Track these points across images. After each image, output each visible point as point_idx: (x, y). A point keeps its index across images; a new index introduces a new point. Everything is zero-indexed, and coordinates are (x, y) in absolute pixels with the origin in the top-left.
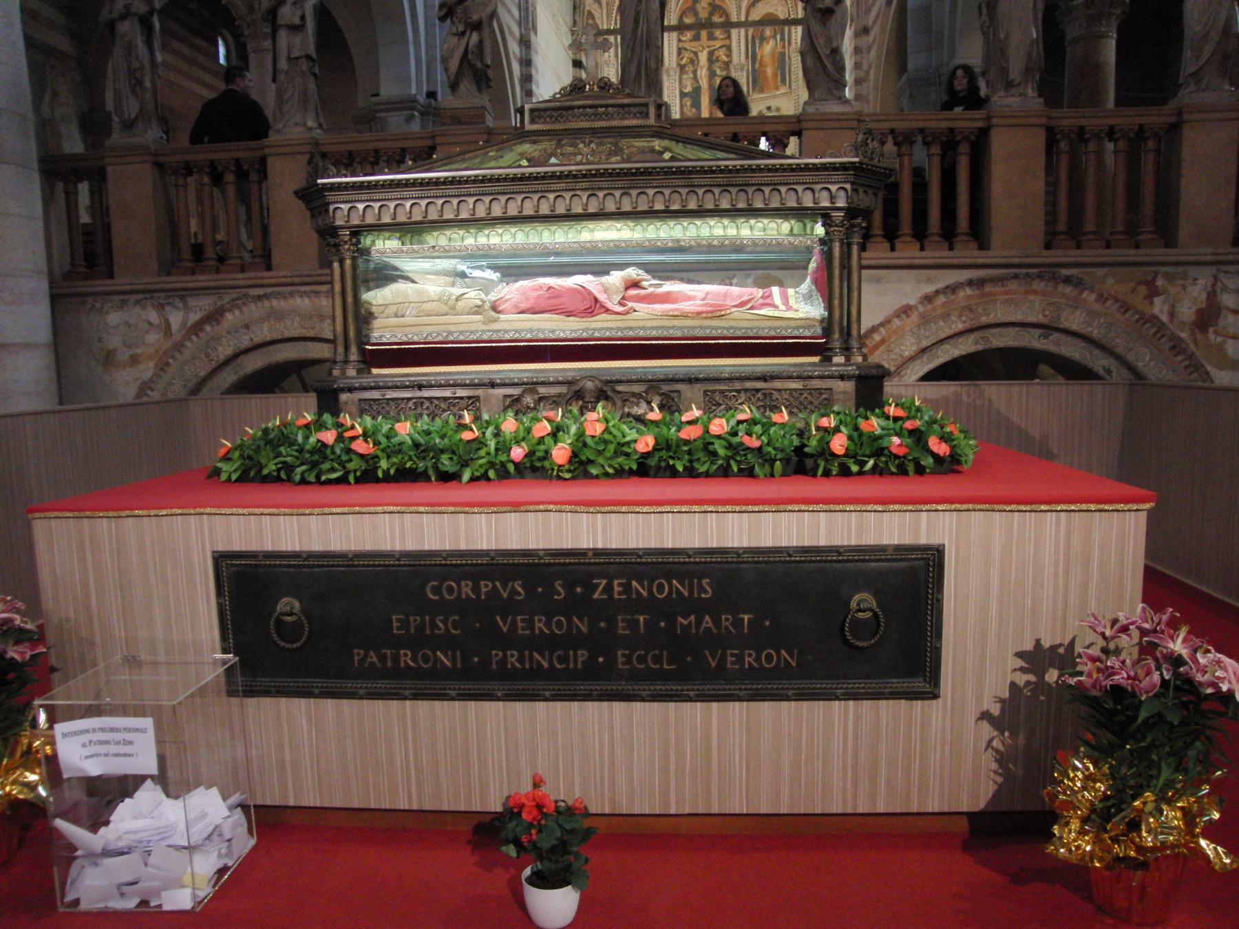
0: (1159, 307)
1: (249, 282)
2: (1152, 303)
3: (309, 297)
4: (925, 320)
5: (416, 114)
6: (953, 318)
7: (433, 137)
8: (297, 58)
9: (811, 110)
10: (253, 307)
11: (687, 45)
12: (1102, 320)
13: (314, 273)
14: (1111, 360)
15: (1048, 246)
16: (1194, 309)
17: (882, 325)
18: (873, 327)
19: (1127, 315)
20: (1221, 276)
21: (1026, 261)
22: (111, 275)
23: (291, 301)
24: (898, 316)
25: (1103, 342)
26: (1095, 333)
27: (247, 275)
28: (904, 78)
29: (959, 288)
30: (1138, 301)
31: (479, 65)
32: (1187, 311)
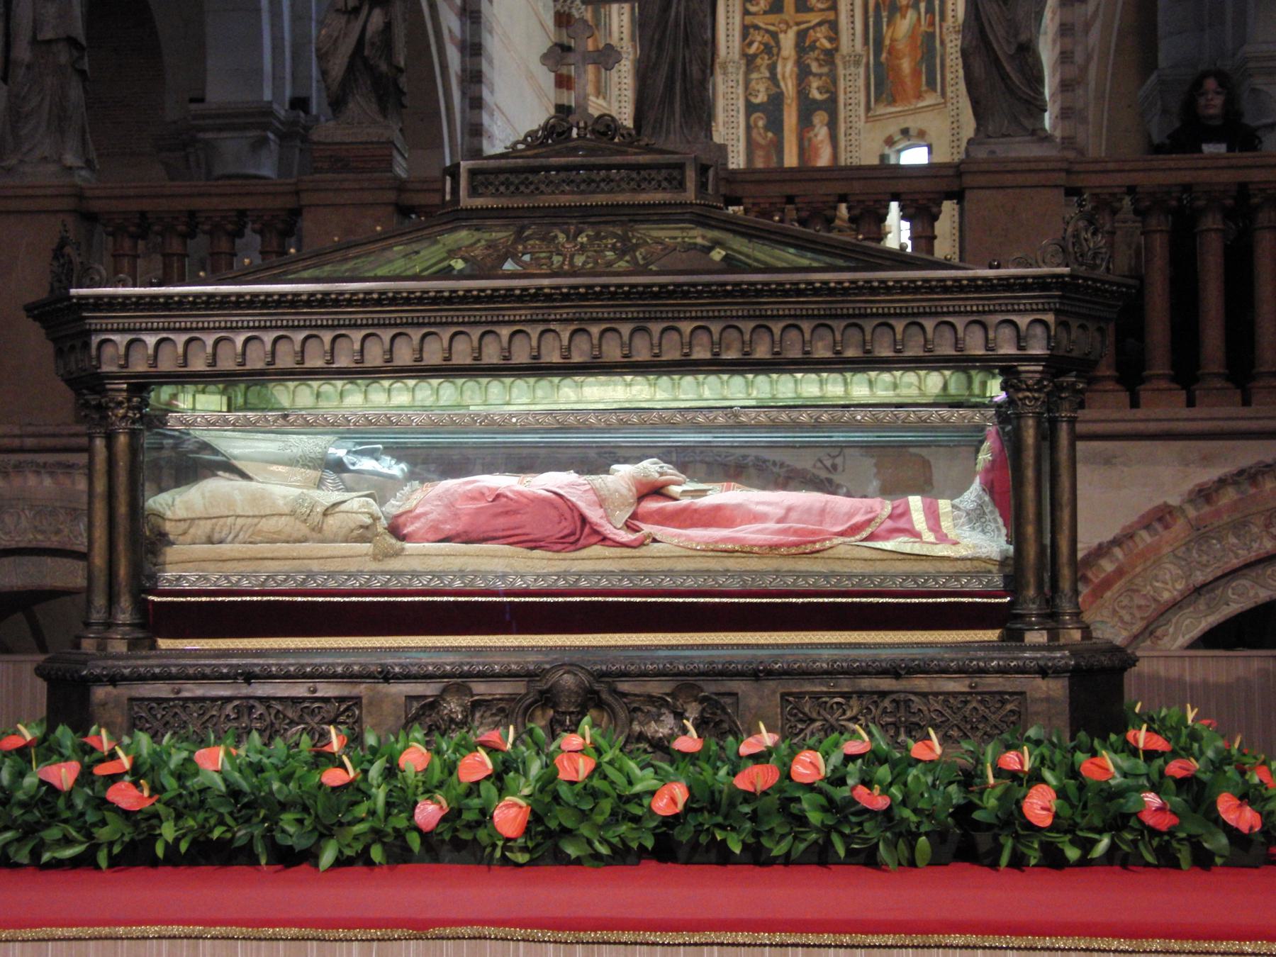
3: (52, 474)
4: (1201, 534)
5: (271, 136)
6: (1255, 530)
7: (297, 193)
8: (49, 42)
9: (981, 153)
11: (759, 21)
17: (1116, 542)
18: (1100, 546)
23: (17, 481)
24: (1147, 527)
28: (1153, 77)
29: (1263, 473)
31: (384, 67)
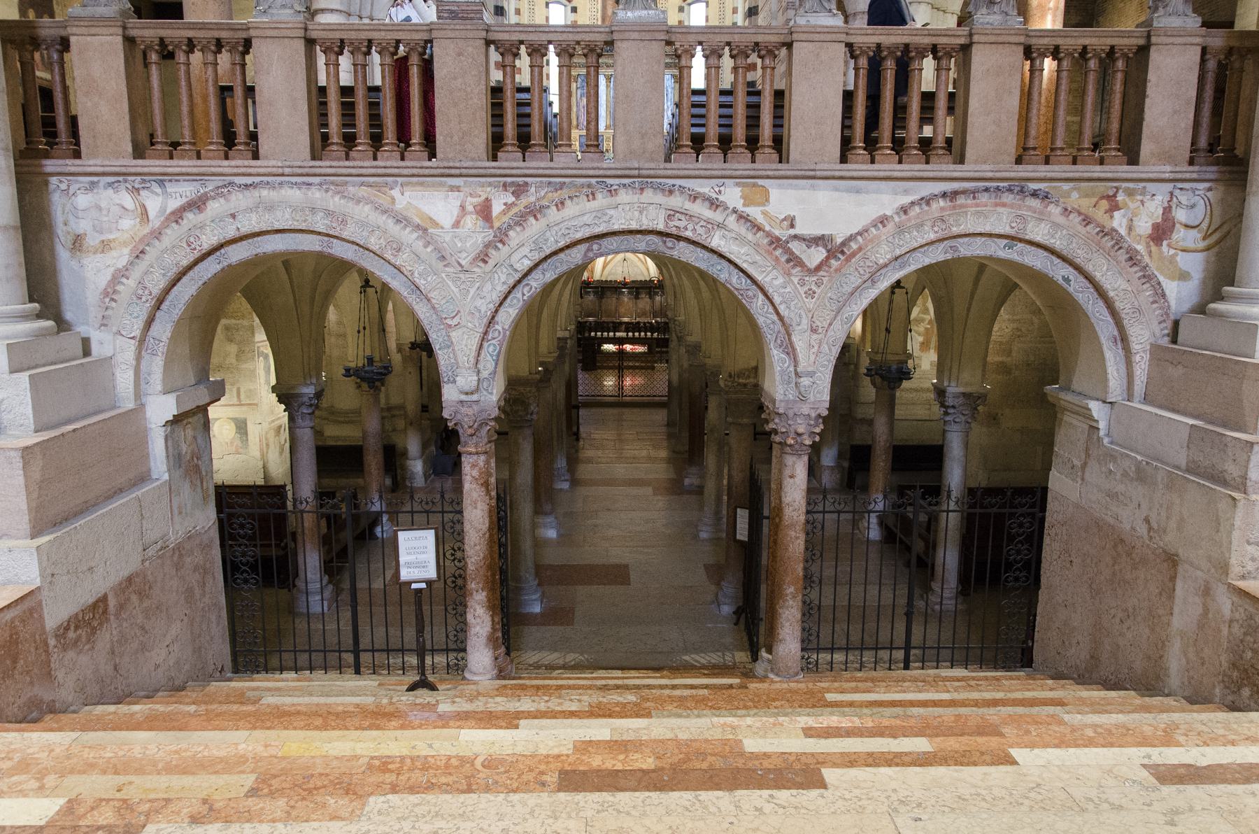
0: (1118, 221)
1: (235, 170)
2: (1112, 217)
3: (300, 189)
10: (240, 196)
12: (1064, 232)
13: (305, 164)
14: (1071, 269)
15: (1019, 161)
16: (1149, 224)
17: (860, 234)
19: (1088, 227)
20: (1177, 192)
21: (998, 175)
22: (77, 155)
23: (283, 192)
24: (875, 226)
25: (1065, 253)
26: (1057, 244)
27: (233, 163)
30: (1099, 214)
32: (1144, 226)
